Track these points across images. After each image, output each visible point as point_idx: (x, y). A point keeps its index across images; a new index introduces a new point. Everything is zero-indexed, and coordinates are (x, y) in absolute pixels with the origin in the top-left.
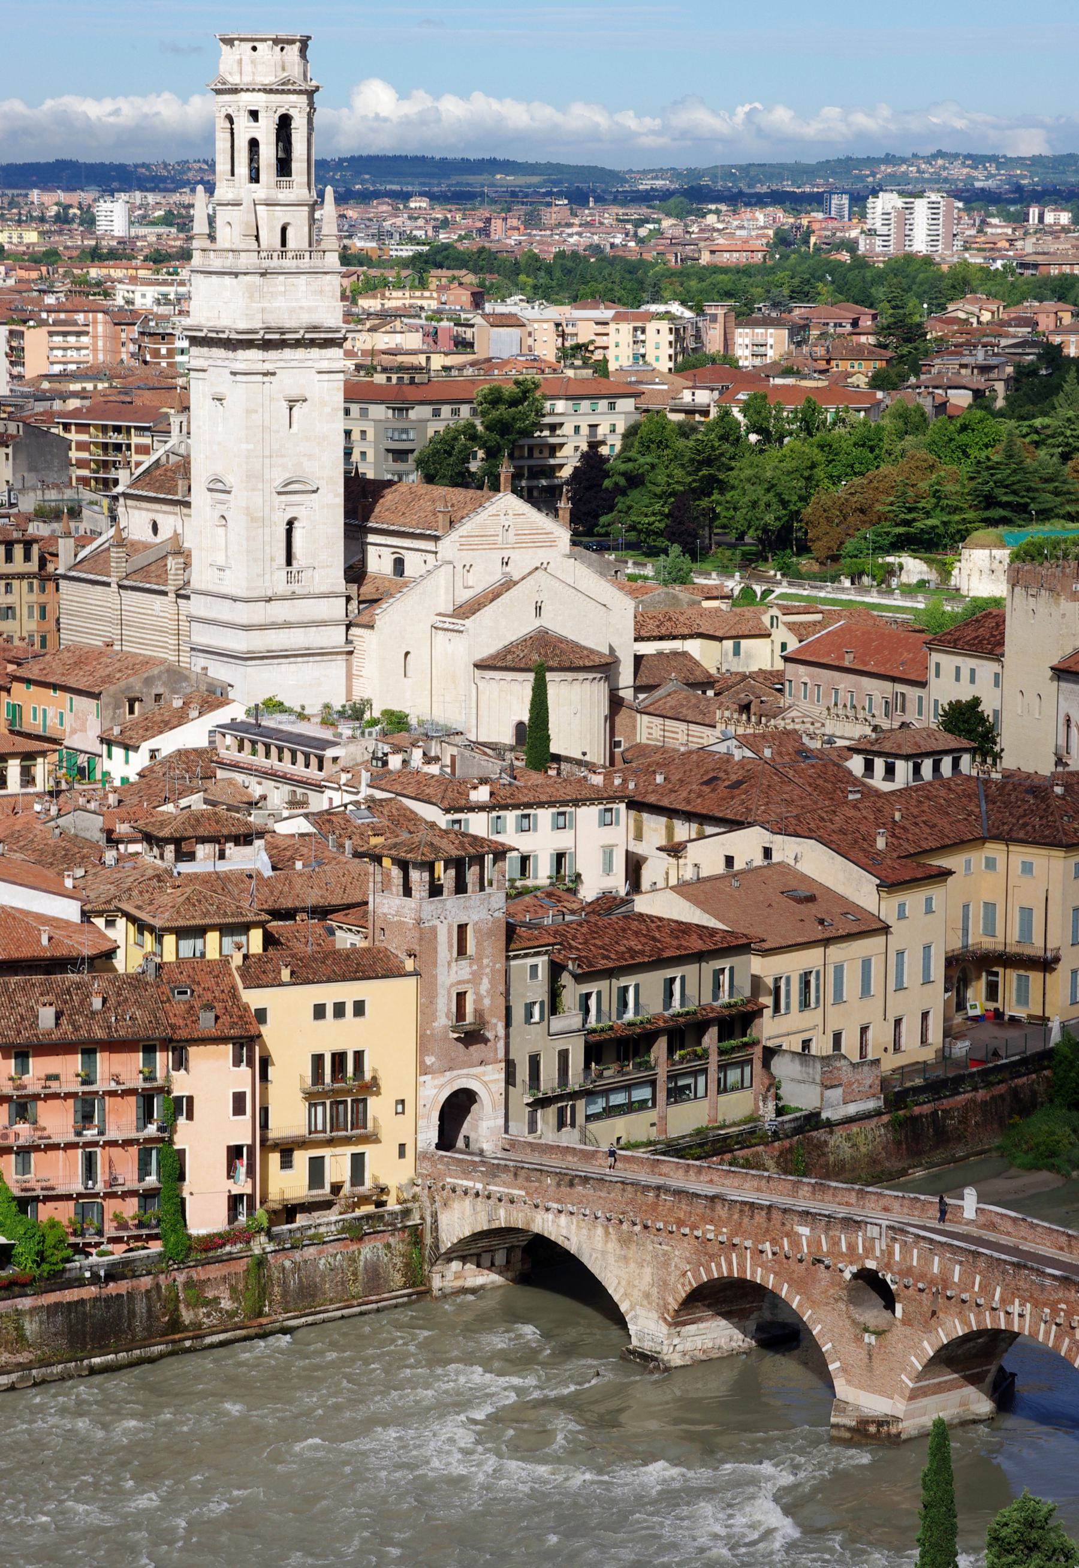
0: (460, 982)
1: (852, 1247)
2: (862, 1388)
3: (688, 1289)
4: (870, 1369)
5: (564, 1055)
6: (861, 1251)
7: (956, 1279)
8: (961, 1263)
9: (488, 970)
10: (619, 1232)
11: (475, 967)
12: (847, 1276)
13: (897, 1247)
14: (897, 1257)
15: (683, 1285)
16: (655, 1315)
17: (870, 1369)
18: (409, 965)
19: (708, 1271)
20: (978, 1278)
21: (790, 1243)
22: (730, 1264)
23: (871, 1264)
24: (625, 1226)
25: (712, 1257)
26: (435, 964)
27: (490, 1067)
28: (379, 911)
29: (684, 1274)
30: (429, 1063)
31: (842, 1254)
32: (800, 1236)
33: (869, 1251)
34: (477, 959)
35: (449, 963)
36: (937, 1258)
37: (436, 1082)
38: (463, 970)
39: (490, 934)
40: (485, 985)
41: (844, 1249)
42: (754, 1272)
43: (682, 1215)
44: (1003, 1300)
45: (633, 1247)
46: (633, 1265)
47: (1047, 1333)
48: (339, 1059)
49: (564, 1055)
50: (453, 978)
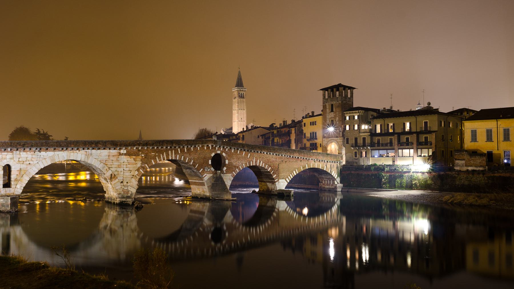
0: (331, 118)
5: (364, 139)
9: (338, 115)
11: (335, 114)
18: (322, 114)
26: (326, 113)
27: (338, 138)
30: (325, 136)
34: (336, 112)
35: (329, 113)
37: (327, 140)
38: (332, 115)
39: (338, 107)
40: (337, 119)
48: (313, 133)
49: (364, 139)
50: (330, 117)
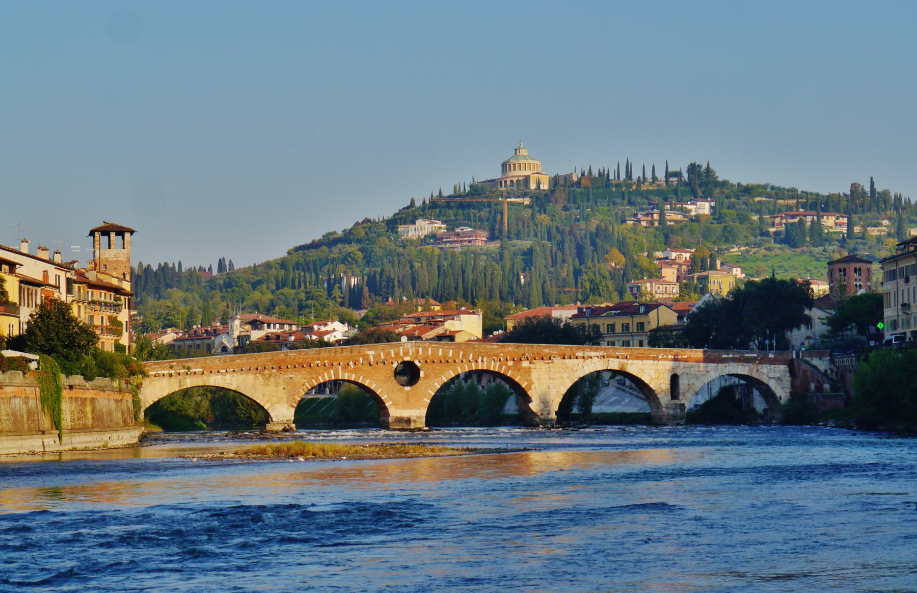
1: (397, 354)
2: (404, 408)
3: (306, 390)
4: (408, 400)
6: (402, 354)
7: (451, 355)
8: (453, 349)
10: (263, 375)
12: (395, 365)
13: (421, 349)
14: (421, 353)
15: (303, 389)
16: (286, 405)
17: (408, 400)
19: (316, 379)
20: (461, 353)
21: (364, 360)
22: (329, 374)
23: (407, 359)
24: (266, 372)
25: (319, 374)
28: (103, 257)
29: (304, 385)
31: (392, 358)
32: (368, 355)
33: (406, 354)
36: (441, 350)
41: (393, 356)
42: (343, 375)
43: (301, 361)
44: (473, 359)
45: (272, 380)
46: (272, 387)
47: (495, 366)
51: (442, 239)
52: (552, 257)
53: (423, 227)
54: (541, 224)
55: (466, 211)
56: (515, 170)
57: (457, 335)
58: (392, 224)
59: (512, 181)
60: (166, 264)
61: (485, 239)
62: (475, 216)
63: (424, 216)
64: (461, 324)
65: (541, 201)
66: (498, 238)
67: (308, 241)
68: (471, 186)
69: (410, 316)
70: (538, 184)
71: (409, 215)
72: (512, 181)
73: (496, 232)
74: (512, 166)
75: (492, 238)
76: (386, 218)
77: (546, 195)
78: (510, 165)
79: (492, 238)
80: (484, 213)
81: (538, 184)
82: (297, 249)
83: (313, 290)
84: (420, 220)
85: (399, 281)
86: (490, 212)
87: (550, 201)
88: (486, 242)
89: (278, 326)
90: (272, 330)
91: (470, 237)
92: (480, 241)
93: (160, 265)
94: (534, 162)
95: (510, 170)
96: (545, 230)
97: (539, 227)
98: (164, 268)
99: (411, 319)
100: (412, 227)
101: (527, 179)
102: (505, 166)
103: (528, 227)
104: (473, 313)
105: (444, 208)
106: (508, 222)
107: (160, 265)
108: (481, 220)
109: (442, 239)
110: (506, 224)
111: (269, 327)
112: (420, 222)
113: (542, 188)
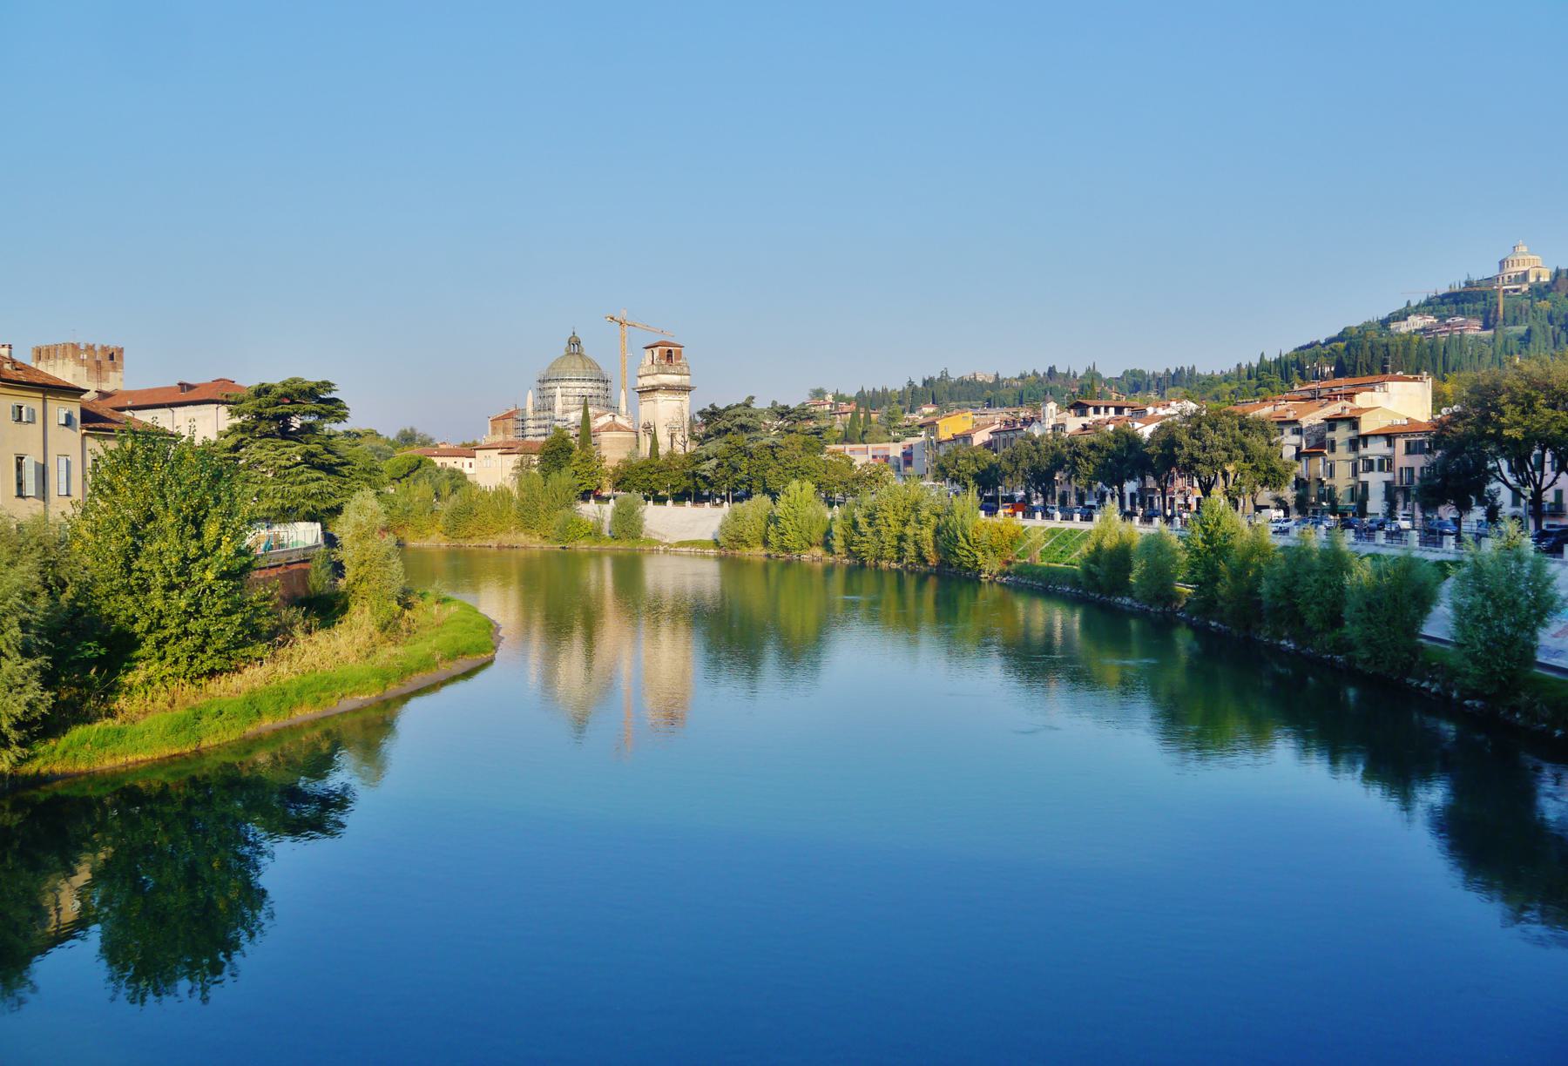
51: (1432, 330)
52: (1554, 338)
53: (1416, 322)
54: (1541, 311)
55: (1460, 305)
56: (1513, 266)
57: (1364, 417)
58: (1385, 323)
59: (1509, 277)
60: (1182, 368)
61: (1478, 328)
62: (1468, 310)
63: (1415, 314)
64: (1389, 398)
65: (1540, 291)
66: (1493, 327)
67: (1306, 342)
68: (1466, 283)
69: (1303, 388)
70: (1538, 277)
71: (1402, 316)
72: (1509, 277)
73: (1491, 321)
74: (1510, 262)
75: (1485, 327)
76: (1380, 319)
77: (1546, 287)
78: (1508, 262)
79: (1485, 327)
80: (1480, 306)
81: (1538, 277)
82: (1296, 350)
83: (1265, 376)
84: (1412, 316)
85: (1367, 365)
86: (1486, 305)
87: (1549, 292)
88: (1480, 330)
89: (1112, 410)
90: (1102, 416)
91: (1462, 326)
92: (1474, 329)
93: (1177, 369)
94: (1533, 257)
95: (1508, 267)
96: (1545, 315)
97: (1539, 312)
98: (1180, 372)
99: (1303, 394)
100: (1403, 324)
101: (1526, 274)
102: (1502, 263)
103: (1527, 314)
104: (1415, 380)
105: (1438, 304)
106: (1504, 310)
107: (1177, 369)
108: (1475, 311)
109: (1432, 330)
110: (1501, 312)
111: (1097, 411)
112: (1411, 319)
113: (1542, 279)
